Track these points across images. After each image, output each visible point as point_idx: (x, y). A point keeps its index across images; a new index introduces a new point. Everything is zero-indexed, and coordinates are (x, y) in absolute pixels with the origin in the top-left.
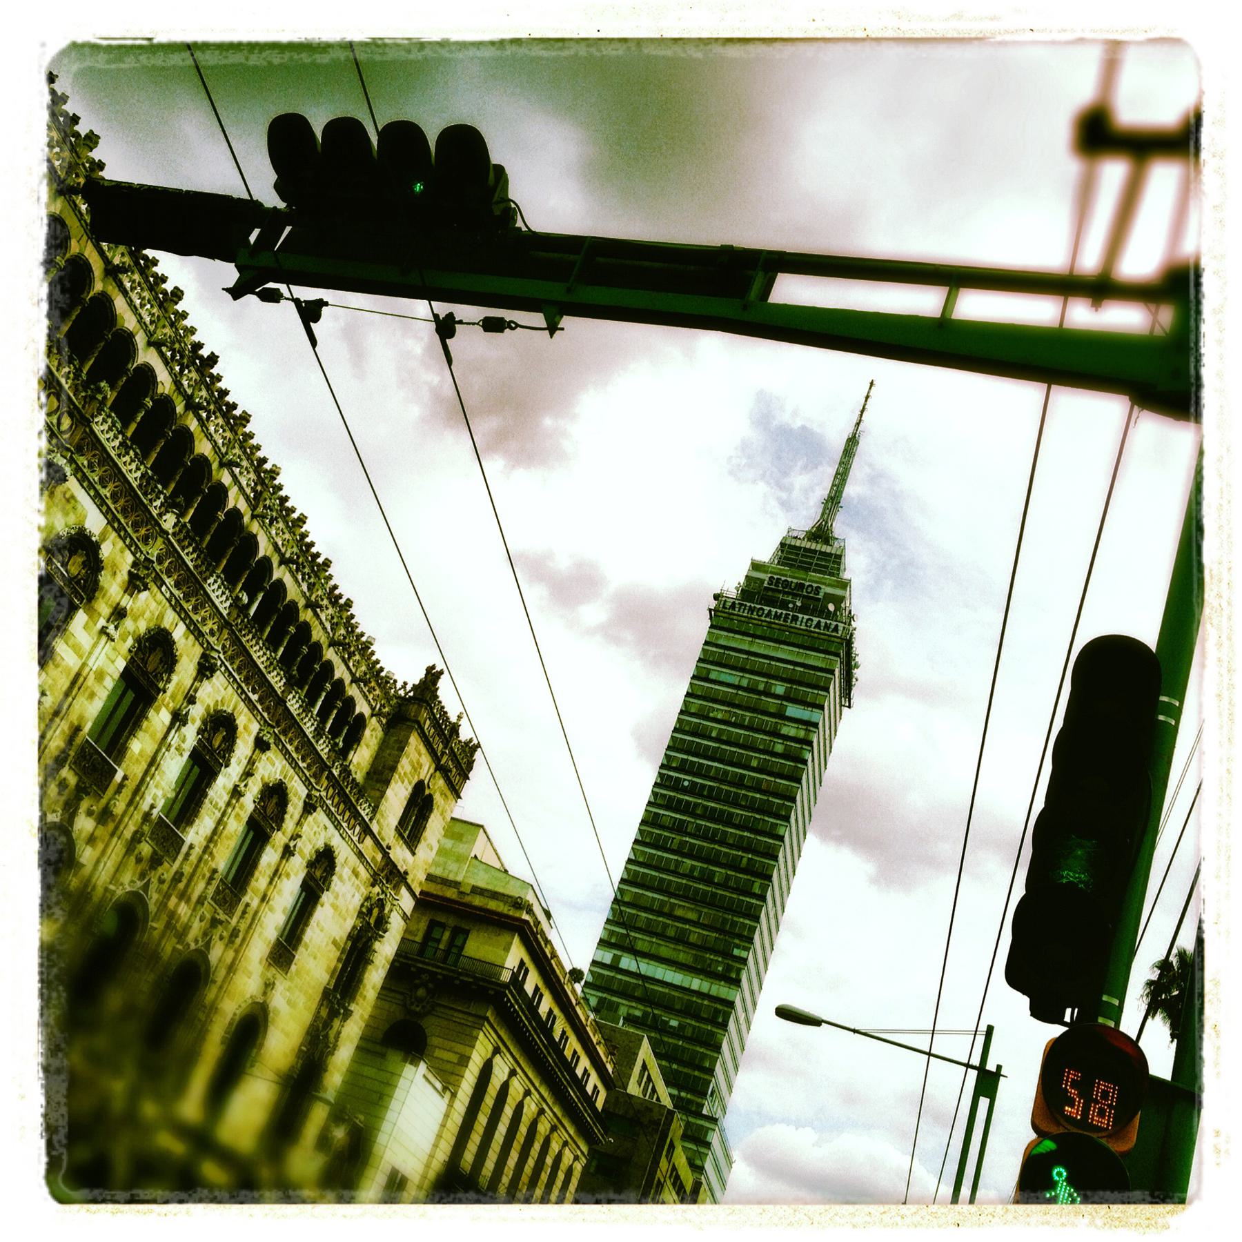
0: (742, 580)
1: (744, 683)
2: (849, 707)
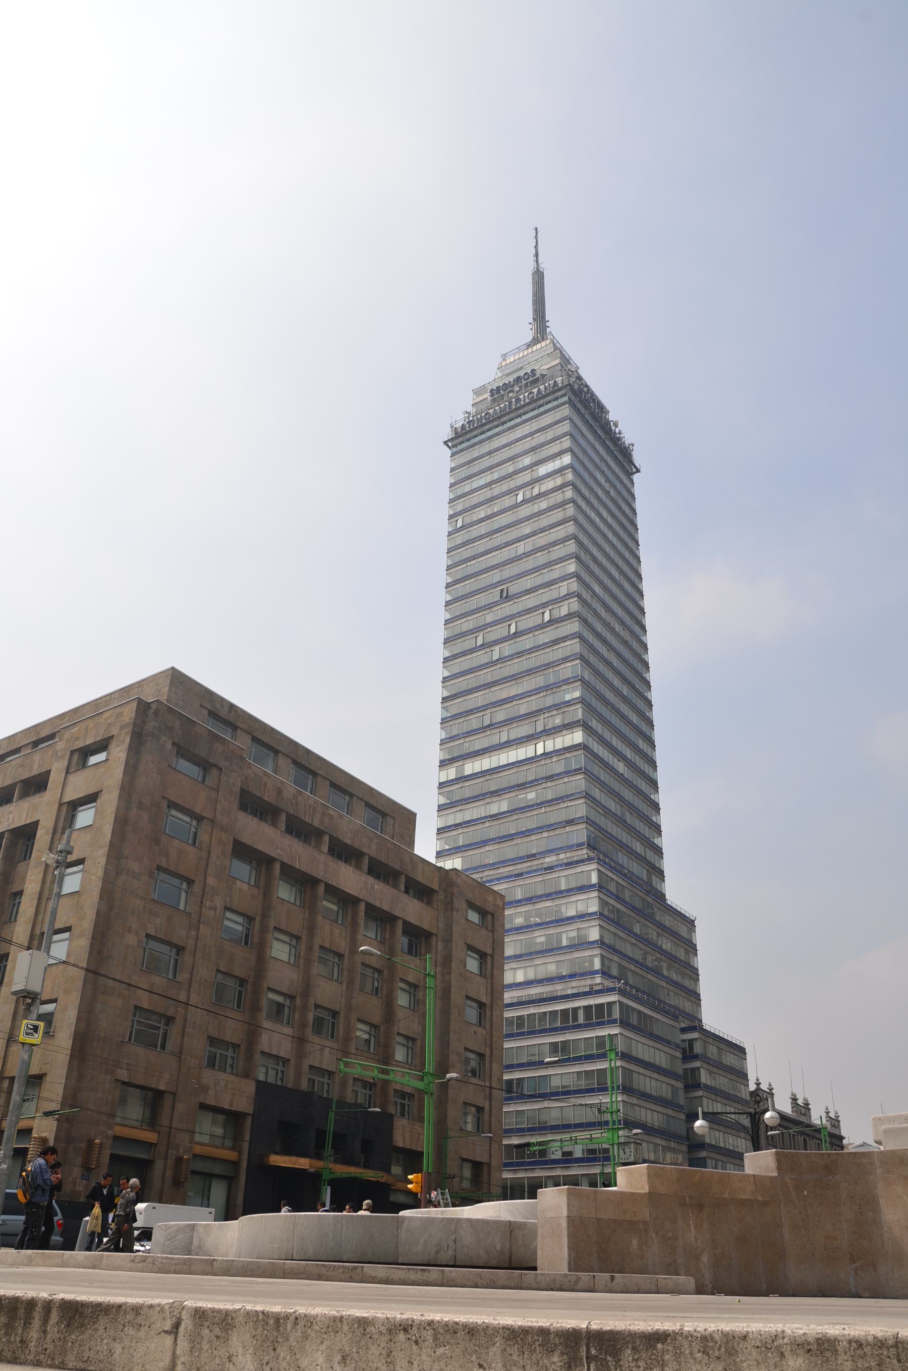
0: (470, 409)
1: (496, 476)
2: (638, 471)
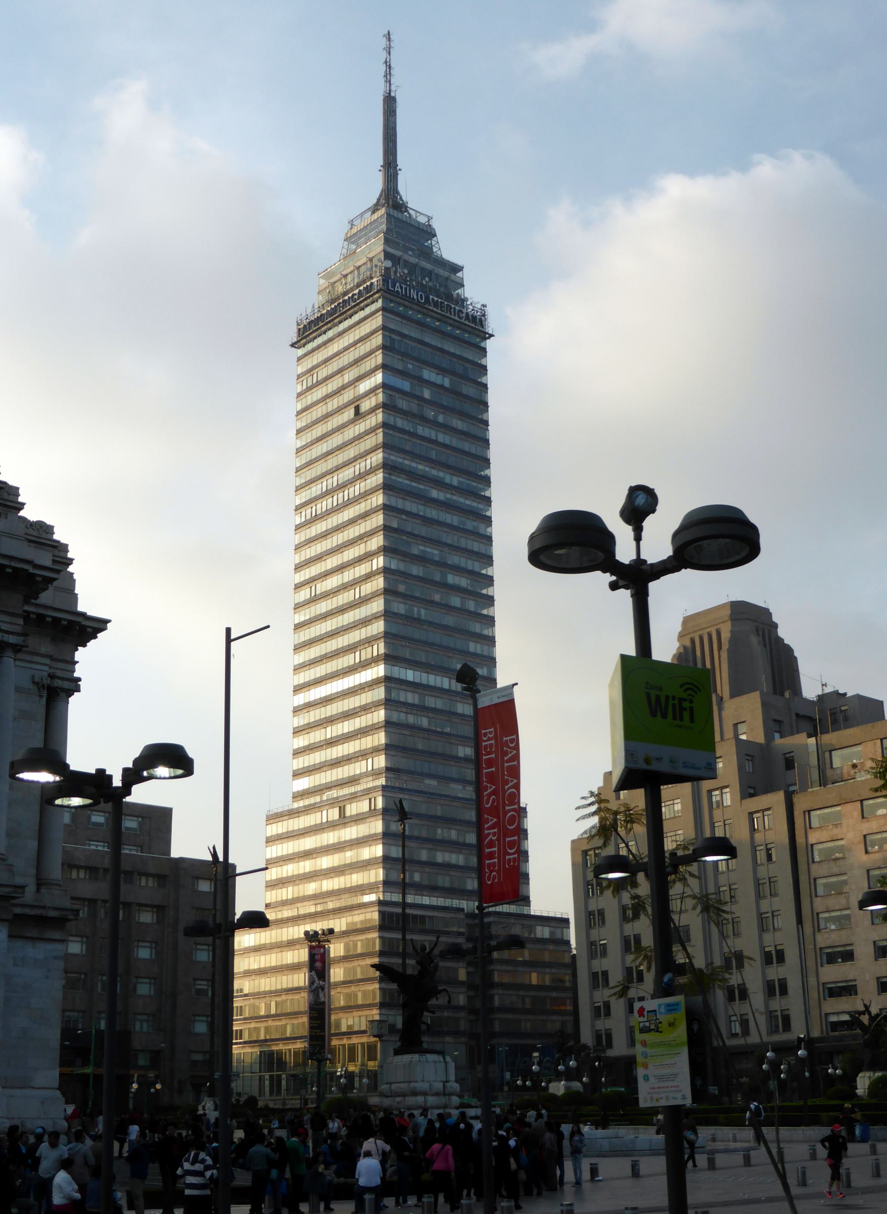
2: (491, 336)
